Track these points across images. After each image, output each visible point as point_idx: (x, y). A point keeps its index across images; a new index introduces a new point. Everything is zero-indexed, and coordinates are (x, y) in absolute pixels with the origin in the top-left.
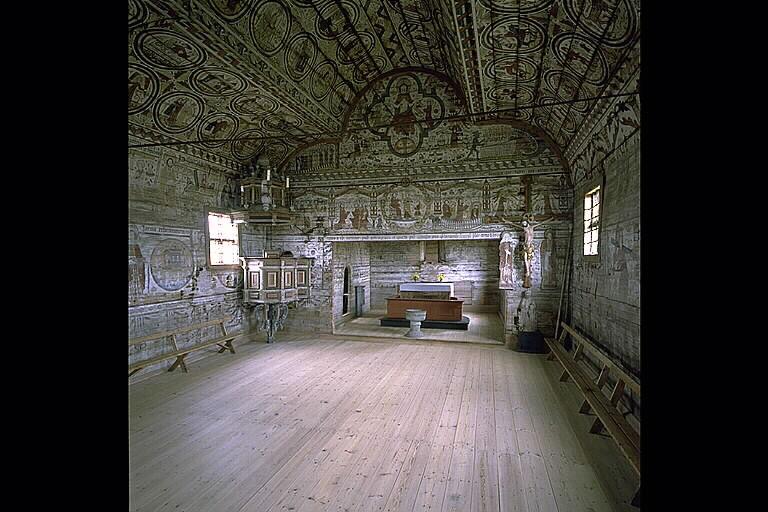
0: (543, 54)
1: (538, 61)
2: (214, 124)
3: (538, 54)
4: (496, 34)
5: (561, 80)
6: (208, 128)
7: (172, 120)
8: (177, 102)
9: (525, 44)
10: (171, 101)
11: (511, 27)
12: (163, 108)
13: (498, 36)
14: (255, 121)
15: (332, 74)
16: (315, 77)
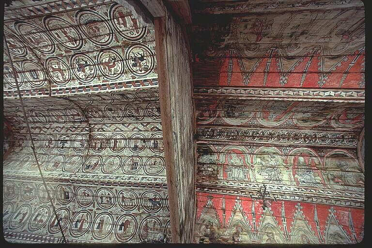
0: (88, 52)
1: (95, 54)
2: (121, 225)
3: (91, 55)
4: (84, 77)
5: (96, 37)
6: (121, 229)
7: (101, 231)
8: (100, 220)
9: (86, 62)
10: (98, 221)
11: (79, 71)
12: (96, 226)
13: (85, 76)
14: (141, 211)
15: (158, 160)
16: (148, 167)
